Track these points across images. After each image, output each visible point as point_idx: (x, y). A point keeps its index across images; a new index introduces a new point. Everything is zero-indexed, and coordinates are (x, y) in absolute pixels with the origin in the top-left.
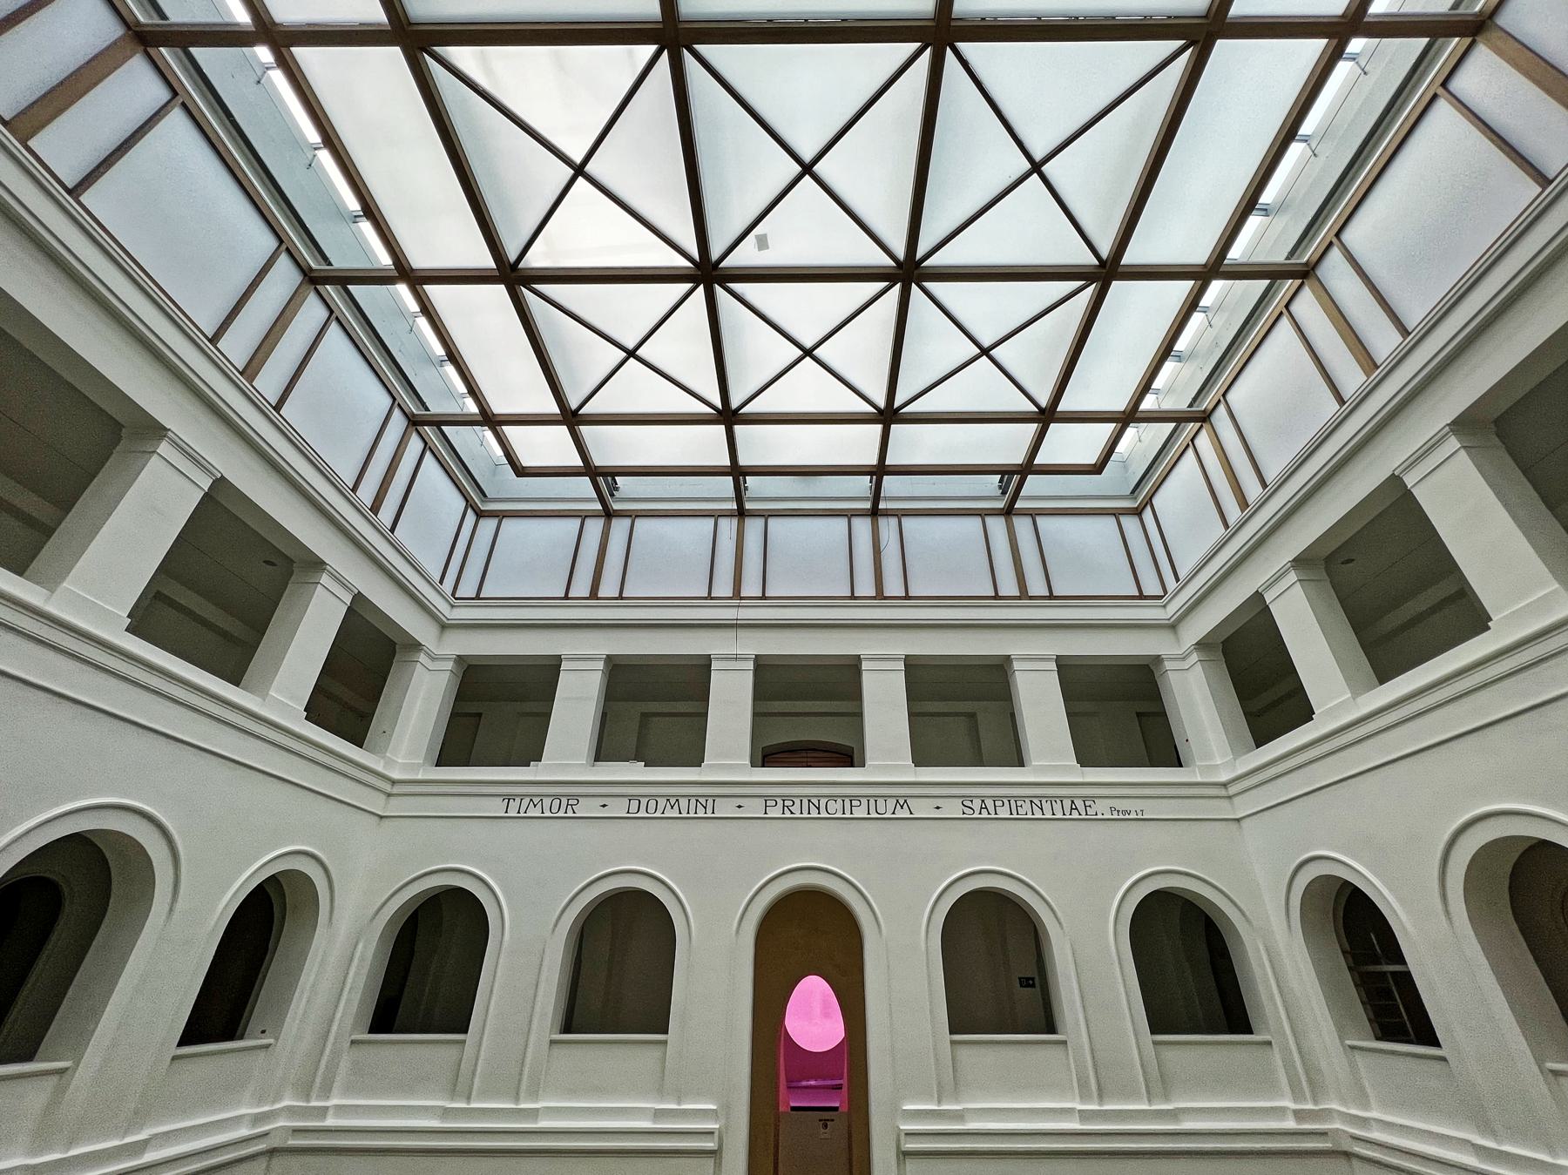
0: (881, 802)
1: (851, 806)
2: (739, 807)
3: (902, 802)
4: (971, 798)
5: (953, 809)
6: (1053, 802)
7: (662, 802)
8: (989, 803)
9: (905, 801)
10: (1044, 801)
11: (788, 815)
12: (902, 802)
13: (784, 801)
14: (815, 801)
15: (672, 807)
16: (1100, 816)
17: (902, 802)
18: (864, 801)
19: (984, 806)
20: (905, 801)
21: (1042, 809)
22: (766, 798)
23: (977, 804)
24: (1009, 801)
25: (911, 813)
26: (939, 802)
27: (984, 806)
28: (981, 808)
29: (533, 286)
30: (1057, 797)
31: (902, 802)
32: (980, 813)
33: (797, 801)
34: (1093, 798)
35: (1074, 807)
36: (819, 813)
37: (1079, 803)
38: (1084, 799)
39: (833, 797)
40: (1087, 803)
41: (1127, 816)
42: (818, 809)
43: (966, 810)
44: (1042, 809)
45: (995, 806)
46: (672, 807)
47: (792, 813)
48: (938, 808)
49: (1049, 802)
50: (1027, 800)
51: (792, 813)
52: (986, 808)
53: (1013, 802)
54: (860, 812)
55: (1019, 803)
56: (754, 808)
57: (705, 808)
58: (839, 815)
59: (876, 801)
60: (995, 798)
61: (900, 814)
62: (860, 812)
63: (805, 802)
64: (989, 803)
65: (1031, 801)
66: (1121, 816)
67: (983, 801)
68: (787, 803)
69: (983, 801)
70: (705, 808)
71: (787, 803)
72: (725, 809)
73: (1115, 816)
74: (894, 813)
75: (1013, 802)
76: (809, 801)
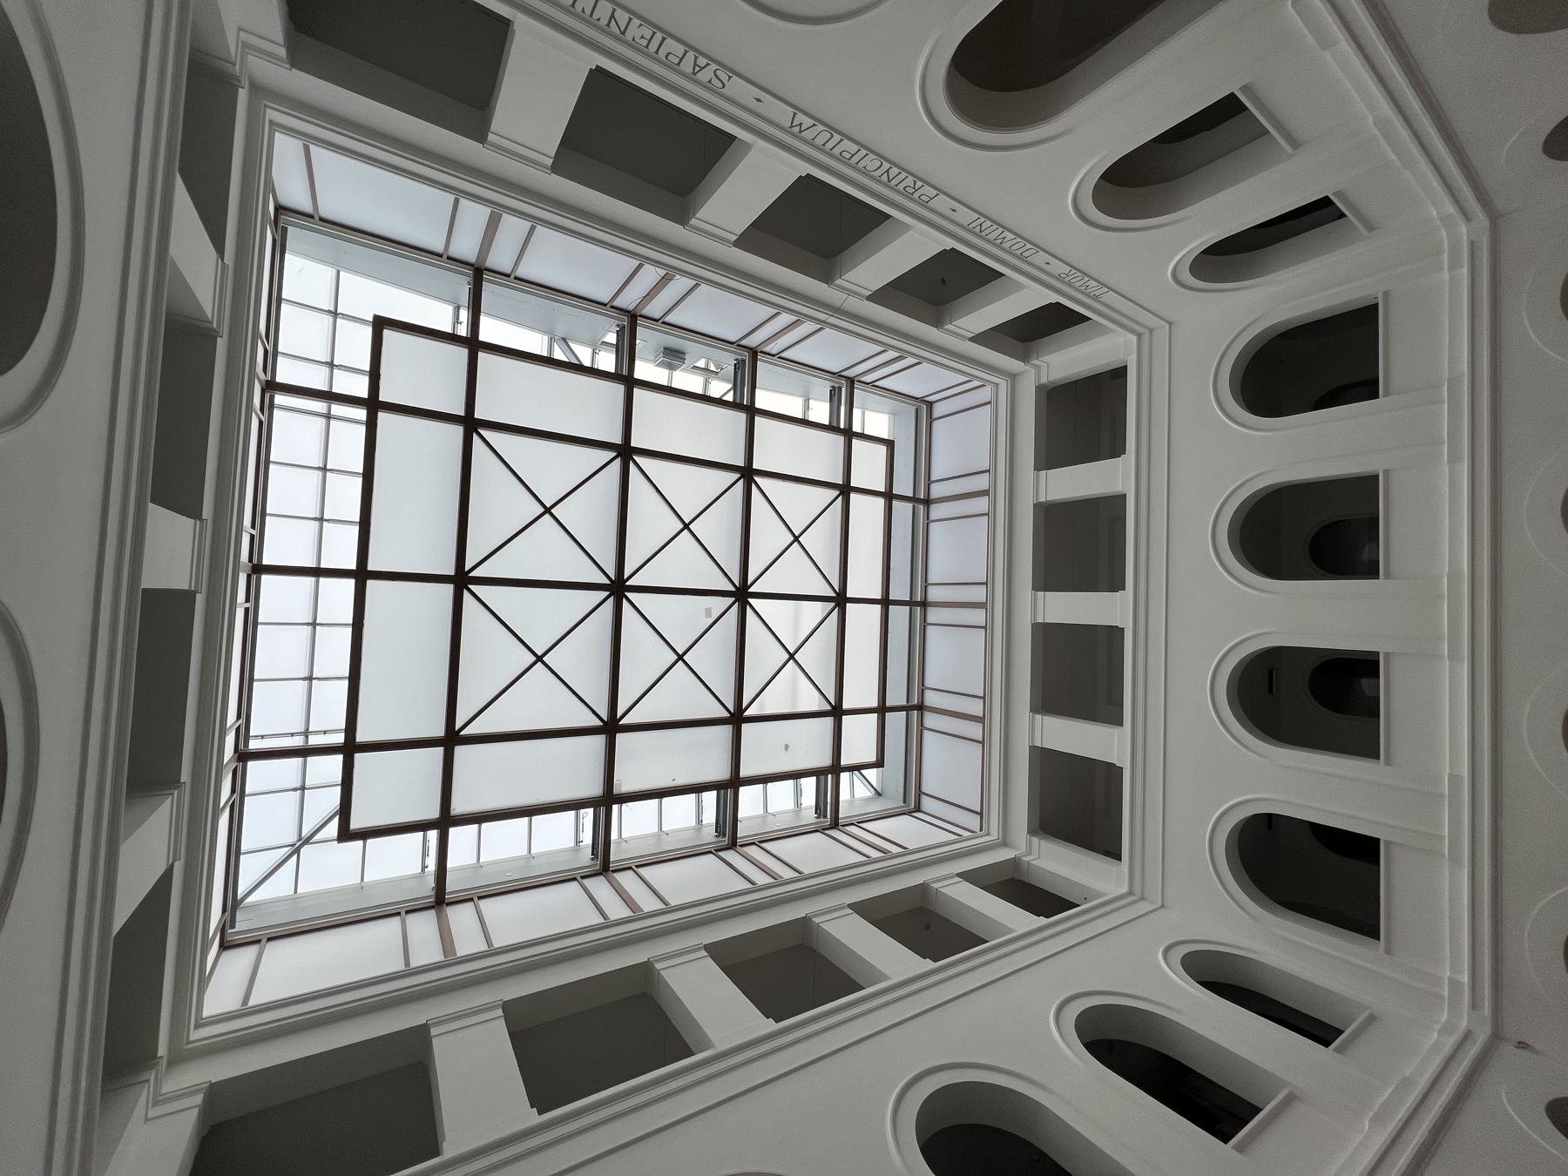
1: (853, 155)
3: (796, 129)
4: (707, 86)
5: (736, 88)
6: (588, 12)
8: (687, 66)
9: (791, 127)
10: (604, 22)
11: (919, 184)
14: (885, 178)
18: (837, 151)
19: (697, 69)
20: (791, 127)
22: (925, 205)
23: (705, 76)
24: (657, 52)
25: (795, 114)
27: (697, 69)
28: (702, 68)
32: (708, 64)
33: (901, 187)
36: (891, 168)
39: (864, 172)
42: (888, 171)
44: (612, 16)
45: (681, 60)
47: (915, 182)
48: (759, 100)
49: (595, 16)
50: (629, 36)
52: (695, 65)
55: (644, 43)
56: (942, 203)
57: (981, 225)
58: (872, 156)
60: (675, 68)
61: (808, 122)
62: (848, 145)
63: (893, 183)
64: (687, 66)
65: (623, 33)
67: (694, 74)
68: (912, 191)
69: (694, 74)
72: (965, 216)
76: (889, 181)
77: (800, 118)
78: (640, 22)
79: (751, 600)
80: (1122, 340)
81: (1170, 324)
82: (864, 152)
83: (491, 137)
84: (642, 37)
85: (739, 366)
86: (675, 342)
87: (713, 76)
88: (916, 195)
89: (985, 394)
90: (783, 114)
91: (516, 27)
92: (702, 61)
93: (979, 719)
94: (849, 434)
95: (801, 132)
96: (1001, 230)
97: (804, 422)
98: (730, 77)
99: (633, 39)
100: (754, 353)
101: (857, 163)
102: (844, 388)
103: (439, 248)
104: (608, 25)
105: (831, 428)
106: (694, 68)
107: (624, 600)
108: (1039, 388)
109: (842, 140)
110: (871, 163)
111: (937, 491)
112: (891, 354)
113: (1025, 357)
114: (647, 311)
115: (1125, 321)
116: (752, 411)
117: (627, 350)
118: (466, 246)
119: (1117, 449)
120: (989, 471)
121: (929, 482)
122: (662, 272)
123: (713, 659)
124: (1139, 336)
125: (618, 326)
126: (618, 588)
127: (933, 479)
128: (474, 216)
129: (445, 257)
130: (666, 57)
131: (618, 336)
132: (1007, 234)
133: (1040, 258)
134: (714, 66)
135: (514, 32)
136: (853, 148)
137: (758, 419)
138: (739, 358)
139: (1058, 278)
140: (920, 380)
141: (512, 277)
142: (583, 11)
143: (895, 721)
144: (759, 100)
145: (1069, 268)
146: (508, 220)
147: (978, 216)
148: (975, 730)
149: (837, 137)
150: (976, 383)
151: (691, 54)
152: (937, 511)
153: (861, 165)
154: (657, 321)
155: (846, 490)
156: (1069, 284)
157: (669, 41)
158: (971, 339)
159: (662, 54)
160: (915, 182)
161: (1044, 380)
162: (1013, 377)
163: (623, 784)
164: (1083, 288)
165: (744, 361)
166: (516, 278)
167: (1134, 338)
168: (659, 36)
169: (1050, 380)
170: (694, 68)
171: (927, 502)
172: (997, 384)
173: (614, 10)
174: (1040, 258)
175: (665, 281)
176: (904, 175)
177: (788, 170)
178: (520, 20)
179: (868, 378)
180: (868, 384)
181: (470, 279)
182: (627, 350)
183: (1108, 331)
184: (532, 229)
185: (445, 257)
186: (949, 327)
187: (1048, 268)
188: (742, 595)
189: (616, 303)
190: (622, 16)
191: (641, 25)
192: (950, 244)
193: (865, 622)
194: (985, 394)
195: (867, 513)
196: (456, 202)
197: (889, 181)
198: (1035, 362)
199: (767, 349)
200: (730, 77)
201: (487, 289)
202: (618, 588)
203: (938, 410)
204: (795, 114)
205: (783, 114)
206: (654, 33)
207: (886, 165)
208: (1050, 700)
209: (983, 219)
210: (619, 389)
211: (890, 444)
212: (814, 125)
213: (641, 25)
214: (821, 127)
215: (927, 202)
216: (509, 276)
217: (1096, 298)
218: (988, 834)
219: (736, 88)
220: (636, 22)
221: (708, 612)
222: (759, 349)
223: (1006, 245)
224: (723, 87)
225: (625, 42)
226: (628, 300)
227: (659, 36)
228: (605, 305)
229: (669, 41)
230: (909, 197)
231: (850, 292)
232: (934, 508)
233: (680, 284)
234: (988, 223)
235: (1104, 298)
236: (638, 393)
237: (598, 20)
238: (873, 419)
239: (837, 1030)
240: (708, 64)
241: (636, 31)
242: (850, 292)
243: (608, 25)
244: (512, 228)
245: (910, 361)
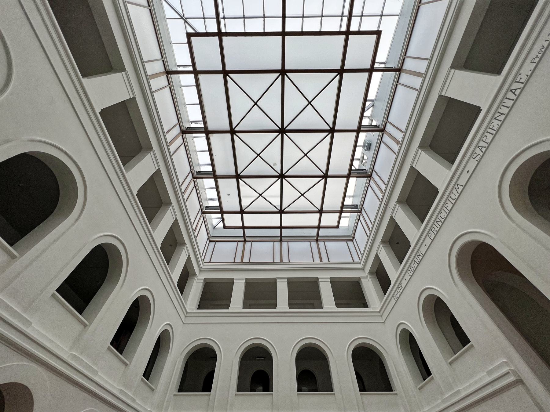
0: (452, 195)
1: (446, 208)
2: (425, 245)
4: (474, 152)
5: (473, 163)
6: (504, 104)
7: (412, 265)
8: (482, 144)
9: (457, 185)
10: (500, 111)
11: (435, 233)
13: (431, 230)
14: (438, 220)
18: (448, 202)
19: (480, 148)
20: (457, 185)
23: (478, 151)
25: (462, 186)
27: (480, 148)
28: (481, 150)
31: (456, 186)
32: (482, 152)
33: (434, 226)
34: (518, 73)
35: (514, 91)
36: (442, 222)
37: (515, 86)
38: (514, 81)
39: (440, 212)
40: (518, 80)
41: (543, 50)
42: (440, 221)
43: (477, 159)
44: (502, 114)
47: (436, 231)
48: (468, 172)
49: (502, 107)
50: (494, 121)
52: (482, 147)
55: (491, 127)
56: (428, 241)
57: (420, 255)
58: (446, 215)
59: (450, 197)
60: (481, 140)
61: (459, 191)
63: (436, 223)
64: (482, 144)
65: (495, 119)
66: (540, 55)
67: (479, 147)
68: (433, 230)
69: (479, 147)
70: (420, 255)
71: (433, 230)
72: (423, 250)
73: (537, 60)
74: (458, 193)
75: (489, 130)
76: (436, 222)
77: (461, 188)
78: (500, 125)
79: (280, 180)
80: (378, 306)
81: (384, 322)
82: (448, 212)
83: (453, 70)
84: (493, 126)
85: (365, 171)
86: (373, 147)
87: (478, 154)
88: (431, 232)
89: (356, 259)
90: (462, 181)
91: (498, 77)
92: (484, 149)
93: (242, 261)
94: (341, 212)
95: (455, 188)
96: (418, 263)
97: (345, 196)
98: (477, 161)
99: (493, 123)
100: (370, 176)
101: (443, 210)
102: (358, 210)
103: (408, 54)
104: (499, 113)
105: (343, 206)
106: (480, 147)
107: (278, 134)
108: (359, 278)
109: (452, 204)
110: (444, 215)
111: (321, 244)
112: (370, 226)
113: (370, 273)
114: (385, 135)
115: (384, 307)
116: (348, 176)
117: (371, 129)
118: (409, 65)
119: (338, 305)
120: (329, 261)
121: (324, 241)
122: (400, 140)
123: (259, 167)
124: (379, 312)
125: (379, 125)
126: (282, 131)
127: (325, 242)
128: (421, 66)
129: (405, 57)
130: (485, 136)
131: (375, 125)
132: (417, 265)
133: (407, 277)
134: (481, 154)
135: (496, 76)
136: (449, 208)
137: (345, 179)
138: (368, 171)
139: (400, 283)
140: (361, 237)
141: (397, 83)
142: (504, 102)
143: (240, 232)
144: (468, 172)
145: (404, 287)
146: (420, 80)
147: (423, 254)
148: (238, 260)
149: (453, 202)
150: (360, 256)
151: (486, 145)
152: (314, 244)
153: (443, 211)
154: (381, 140)
155: (321, 212)
156: (398, 287)
157: (492, 136)
158: (377, 254)
159: (486, 134)
160: (436, 231)
161: (362, 280)
162: (363, 269)
163: (213, 137)
164: (396, 292)
165: (367, 173)
166: (397, 85)
167: (378, 310)
168: (494, 132)
169: (363, 282)
170: (480, 147)
171: (317, 241)
172: (360, 264)
173: (504, 114)
174: (407, 277)
175: (397, 142)
176: (439, 227)
177: (441, 186)
178: (499, 79)
179: (361, 218)
180: (359, 218)
181: (396, 67)
182: (371, 129)
183: (381, 301)
184: (417, 90)
185: (405, 57)
186: (381, 246)
187: (404, 279)
188: (282, 176)
189: (388, 124)
190: (502, 118)
191: (498, 125)
192: (413, 245)
193: (274, 219)
194: (356, 259)
195: (313, 220)
196: (427, 59)
198: (369, 276)
199: (371, 181)
200: (477, 161)
201: (392, 74)
202: (282, 131)
203: (350, 243)
204: (462, 186)
205: (462, 181)
206: (495, 130)
207: (442, 220)
208: (250, 284)
209: (422, 256)
210: (355, 127)
211: (337, 227)
212: (458, 193)
213: (498, 125)
214: (457, 196)
216: (398, 82)
217: (393, 297)
218: (203, 265)
219: (473, 163)
220: (500, 123)
221: (275, 164)
222: (371, 178)
223: (412, 265)
224: (473, 158)
225: (491, 120)
226: (389, 128)
227: (494, 132)
228: (387, 120)
229: (492, 136)
230: (430, 229)
231: (394, 210)
232: (315, 243)
233: (396, 147)
234: (420, 258)
235: (393, 300)
236: (354, 134)
237: (501, 109)
238: (346, 220)
240: (482, 152)
241: (496, 123)
242: (394, 210)
243: (499, 113)
244: (417, 82)
245: (368, 233)
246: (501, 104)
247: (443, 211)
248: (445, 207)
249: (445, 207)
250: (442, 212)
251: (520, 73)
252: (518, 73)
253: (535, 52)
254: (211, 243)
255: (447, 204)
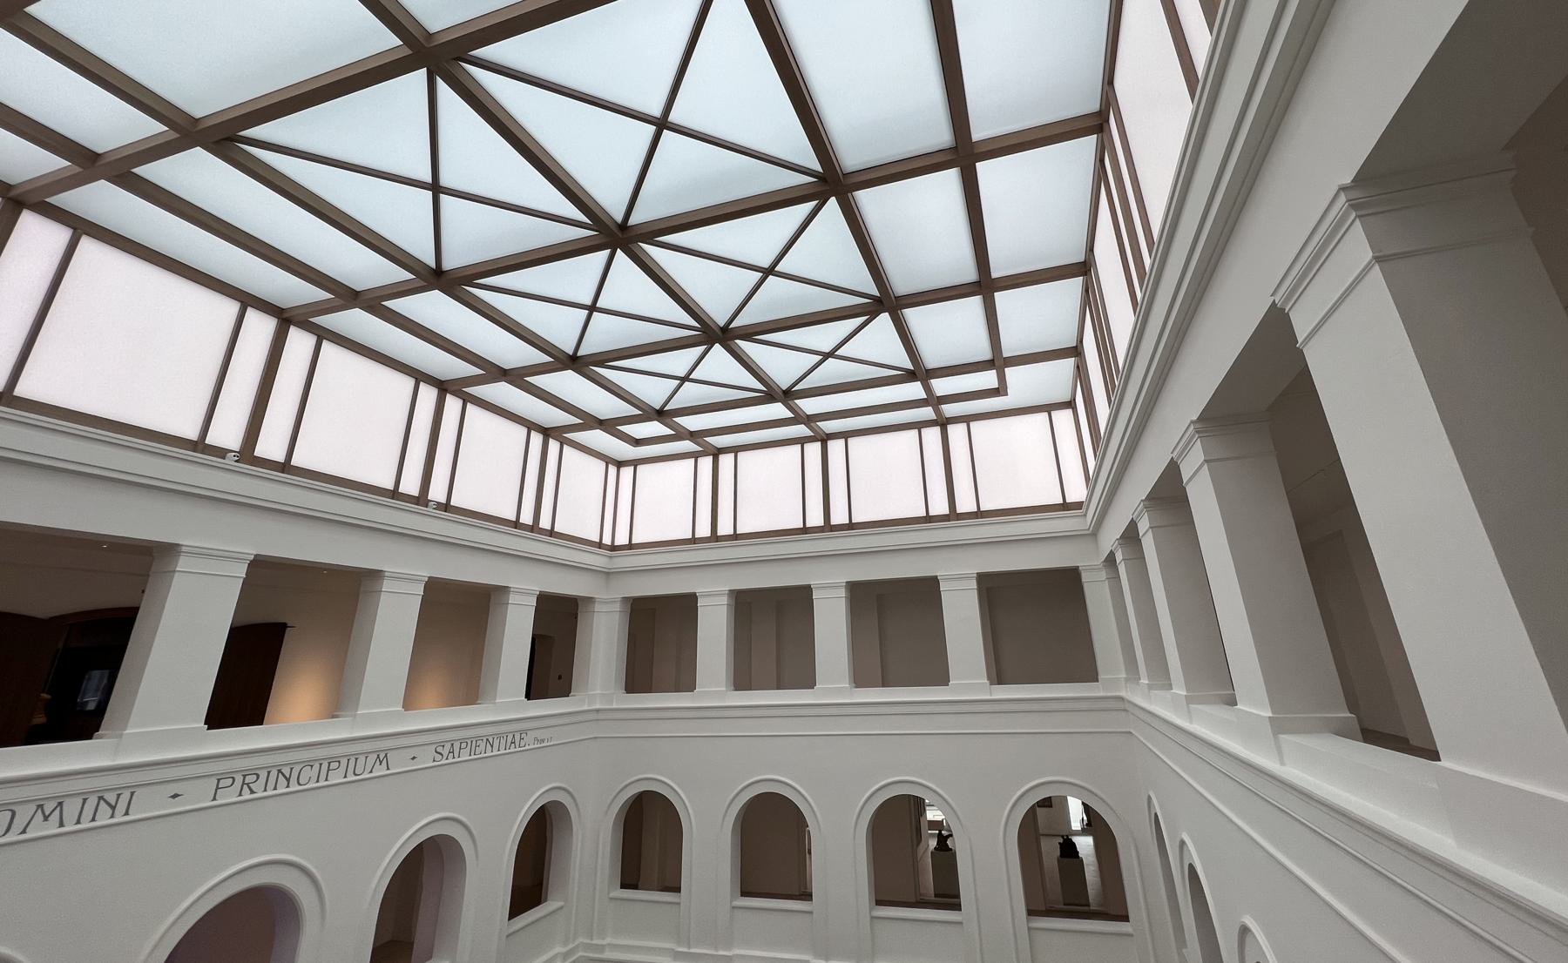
0: (362, 759)
9: (386, 756)
11: (247, 796)
12: (382, 758)
13: (244, 776)
14: (286, 771)
15: (46, 818)
16: (527, 747)
17: (382, 758)
20: (386, 756)
21: (492, 746)
23: (448, 746)
26: (412, 752)
29: (241, 133)
30: (496, 735)
33: (263, 775)
34: (525, 731)
42: (288, 780)
44: (492, 746)
46: (46, 818)
47: (252, 792)
48: (414, 758)
50: (485, 740)
51: (252, 792)
52: (453, 752)
53: (474, 742)
54: (336, 778)
56: (198, 796)
63: (274, 773)
68: (249, 779)
71: (249, 779)
75: (474, 742)
76: (280, 771)
88: (239, 779)
197: (280, 771)
207: (294, 787)
215: (219, 780)
239: (1345, 238)
246: (499, 736)
247: (316, 766)
248: (329, 763)
249: (329, 763)
250: (312, 766)
251: (528, 732)
252: (525, 731)
253: (540, 734)
254: (623, 470)
255: (337, 764)
